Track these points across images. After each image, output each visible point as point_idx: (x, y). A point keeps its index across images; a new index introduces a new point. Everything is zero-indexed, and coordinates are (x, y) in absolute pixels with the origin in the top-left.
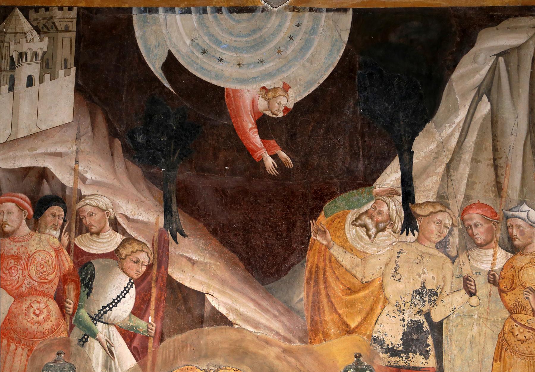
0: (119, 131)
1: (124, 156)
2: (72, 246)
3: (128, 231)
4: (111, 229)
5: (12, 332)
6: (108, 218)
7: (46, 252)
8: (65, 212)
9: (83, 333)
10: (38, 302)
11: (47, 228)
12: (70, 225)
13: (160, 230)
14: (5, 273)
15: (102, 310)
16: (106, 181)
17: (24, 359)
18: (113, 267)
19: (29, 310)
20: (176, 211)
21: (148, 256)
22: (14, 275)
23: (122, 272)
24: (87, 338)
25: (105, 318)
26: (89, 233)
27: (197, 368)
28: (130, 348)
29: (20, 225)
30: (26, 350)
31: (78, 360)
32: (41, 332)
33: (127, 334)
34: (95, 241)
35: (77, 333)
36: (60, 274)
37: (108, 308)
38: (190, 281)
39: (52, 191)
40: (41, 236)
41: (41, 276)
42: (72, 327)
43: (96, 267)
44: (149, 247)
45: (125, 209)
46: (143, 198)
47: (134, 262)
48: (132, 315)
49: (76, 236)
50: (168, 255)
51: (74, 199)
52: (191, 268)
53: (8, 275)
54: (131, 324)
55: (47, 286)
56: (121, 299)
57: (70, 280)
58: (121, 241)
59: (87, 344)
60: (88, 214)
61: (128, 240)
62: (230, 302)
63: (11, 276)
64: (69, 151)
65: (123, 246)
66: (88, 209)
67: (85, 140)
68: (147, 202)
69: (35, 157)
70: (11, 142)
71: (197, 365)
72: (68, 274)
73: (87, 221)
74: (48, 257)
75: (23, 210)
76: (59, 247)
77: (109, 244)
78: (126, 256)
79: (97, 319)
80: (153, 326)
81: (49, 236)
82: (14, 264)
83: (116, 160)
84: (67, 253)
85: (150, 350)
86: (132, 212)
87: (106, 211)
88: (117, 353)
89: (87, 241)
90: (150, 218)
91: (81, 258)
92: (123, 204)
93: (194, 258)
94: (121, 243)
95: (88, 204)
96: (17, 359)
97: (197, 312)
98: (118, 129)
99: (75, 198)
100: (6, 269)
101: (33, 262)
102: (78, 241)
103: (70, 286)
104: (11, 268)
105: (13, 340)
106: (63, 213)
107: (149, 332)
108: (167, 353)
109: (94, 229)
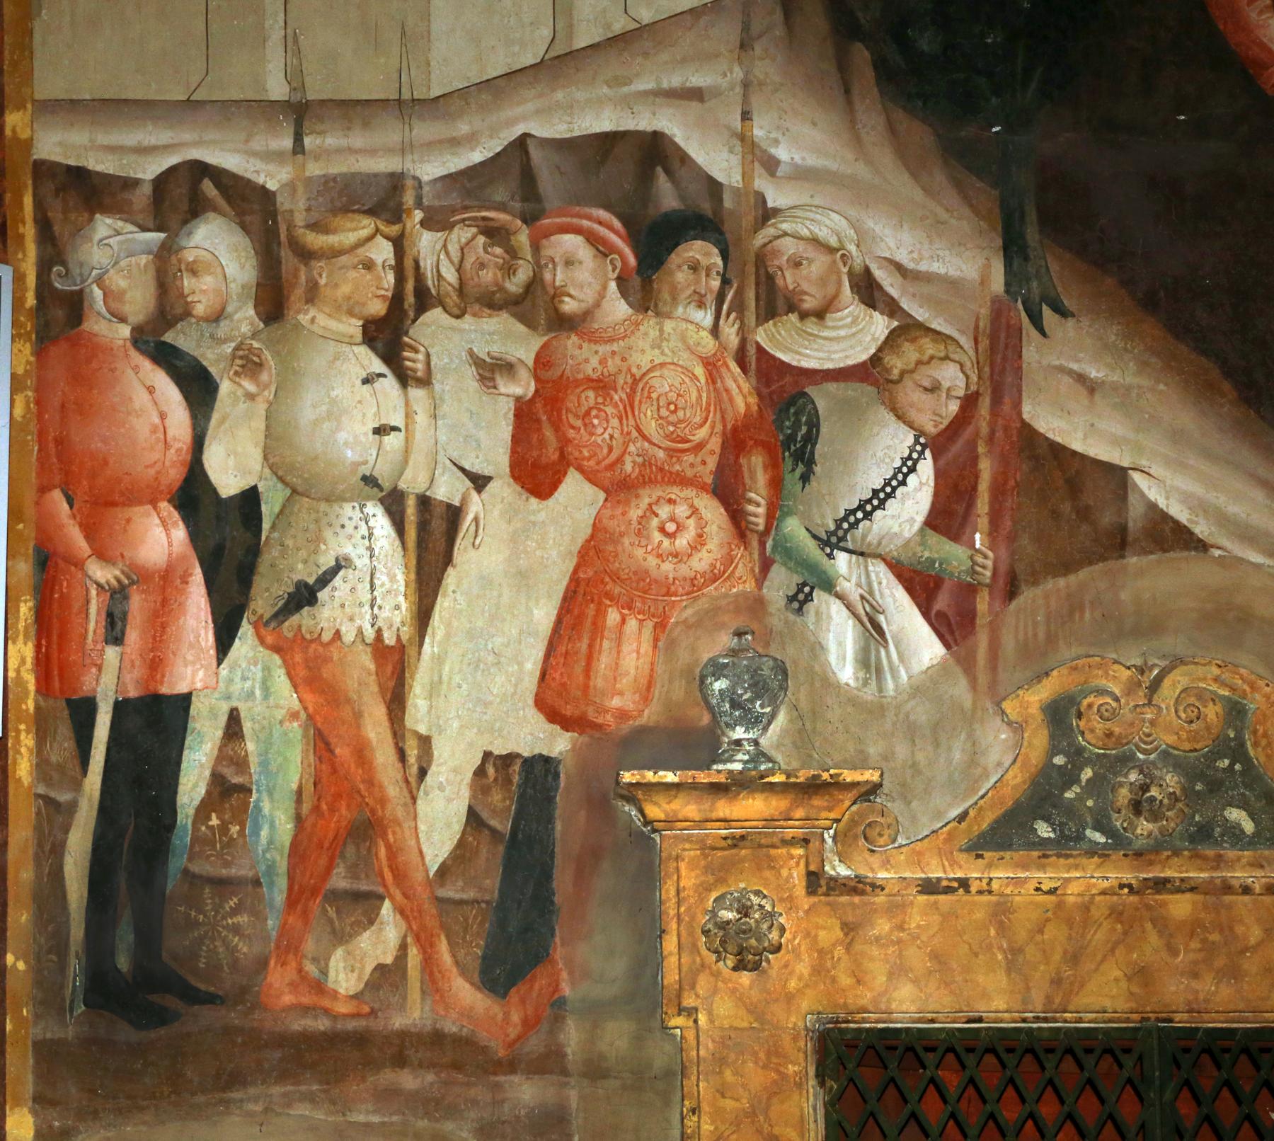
0: (863, 21)
2: (752, 351)
4: (856, 302)
5: (607, 579)
6: (845, 270)
8: (725, 256)
9: (797, 579)
10: (670, 501)
12: (740, 293)
13: (995, 301)
14: (573, 427)
15: (845, 519)
16: (832, 165)
17: (646, 647)
19: (648, 522)
21: (963, 372)
22: (600, 430)
23: (894, 418)
24: (811, 593)
25: (854, 540)
26: (796, 314)
27: (1116, 662)
28: (926, 614)
29: (602, 295)
30: (649, 625)
31: (791, 650)
32: (685, 579)
33: (917, 579)
34: (811, 334)
35: (781, 582)
36: (725, 426)
37: (860, 515)
39: (682, 198)
40: (661, 325)
42: (766, 565)
43: (821, 405)
44: (966, 347)
45: (892, 245)
46: (944, 215)
47: (926, 389)
48: (929, 532)
50: (1020, 368)
51: (747, 221)
52: (1086, 402)
53: (582, 431)
54: (927, 554)
55: (689, 458)
56: (894, 489)
57: (751, 443)
58: (887, 332)
59: (810, 608)
60: (788, 260)
61: (907, 330)
62: (1197, 489)
63: (592, 434)
64: (724, 83)
66: (789, 247)
67: (766, 50)
68: (953, 221)
69: (627, 103)
70: (556, 62)
71: (1114, 656)
72: (746, 427)
73: (789, 279)
74: (687, 380)
75: (606, 256)
76: (715, 354)
77: (853, 341)
78: (903, 373)
79: (832, 541)
80: (986, 557)
81: (684, 325)
82: (597, 403)
83: (859, 107)
84: (739, 370)
86: (912, 252)
87: (838, 250)
88: (894, 628)
89: (791, 336)
90: (964, 267)
92: (887, 231)
93: (1093, 374)
94: (887, 338)
95: (785, 234)
96: (628, 648)
97: (1107, 519)
98: (860, 14)
99: (751, 218)
100: (577, 416)
101: (646, 394)
103: (753, 458)
104: (588, 413)
106: (719, 261)
107: (977, 573)
108: (1030, 629)
109: (809, 303)
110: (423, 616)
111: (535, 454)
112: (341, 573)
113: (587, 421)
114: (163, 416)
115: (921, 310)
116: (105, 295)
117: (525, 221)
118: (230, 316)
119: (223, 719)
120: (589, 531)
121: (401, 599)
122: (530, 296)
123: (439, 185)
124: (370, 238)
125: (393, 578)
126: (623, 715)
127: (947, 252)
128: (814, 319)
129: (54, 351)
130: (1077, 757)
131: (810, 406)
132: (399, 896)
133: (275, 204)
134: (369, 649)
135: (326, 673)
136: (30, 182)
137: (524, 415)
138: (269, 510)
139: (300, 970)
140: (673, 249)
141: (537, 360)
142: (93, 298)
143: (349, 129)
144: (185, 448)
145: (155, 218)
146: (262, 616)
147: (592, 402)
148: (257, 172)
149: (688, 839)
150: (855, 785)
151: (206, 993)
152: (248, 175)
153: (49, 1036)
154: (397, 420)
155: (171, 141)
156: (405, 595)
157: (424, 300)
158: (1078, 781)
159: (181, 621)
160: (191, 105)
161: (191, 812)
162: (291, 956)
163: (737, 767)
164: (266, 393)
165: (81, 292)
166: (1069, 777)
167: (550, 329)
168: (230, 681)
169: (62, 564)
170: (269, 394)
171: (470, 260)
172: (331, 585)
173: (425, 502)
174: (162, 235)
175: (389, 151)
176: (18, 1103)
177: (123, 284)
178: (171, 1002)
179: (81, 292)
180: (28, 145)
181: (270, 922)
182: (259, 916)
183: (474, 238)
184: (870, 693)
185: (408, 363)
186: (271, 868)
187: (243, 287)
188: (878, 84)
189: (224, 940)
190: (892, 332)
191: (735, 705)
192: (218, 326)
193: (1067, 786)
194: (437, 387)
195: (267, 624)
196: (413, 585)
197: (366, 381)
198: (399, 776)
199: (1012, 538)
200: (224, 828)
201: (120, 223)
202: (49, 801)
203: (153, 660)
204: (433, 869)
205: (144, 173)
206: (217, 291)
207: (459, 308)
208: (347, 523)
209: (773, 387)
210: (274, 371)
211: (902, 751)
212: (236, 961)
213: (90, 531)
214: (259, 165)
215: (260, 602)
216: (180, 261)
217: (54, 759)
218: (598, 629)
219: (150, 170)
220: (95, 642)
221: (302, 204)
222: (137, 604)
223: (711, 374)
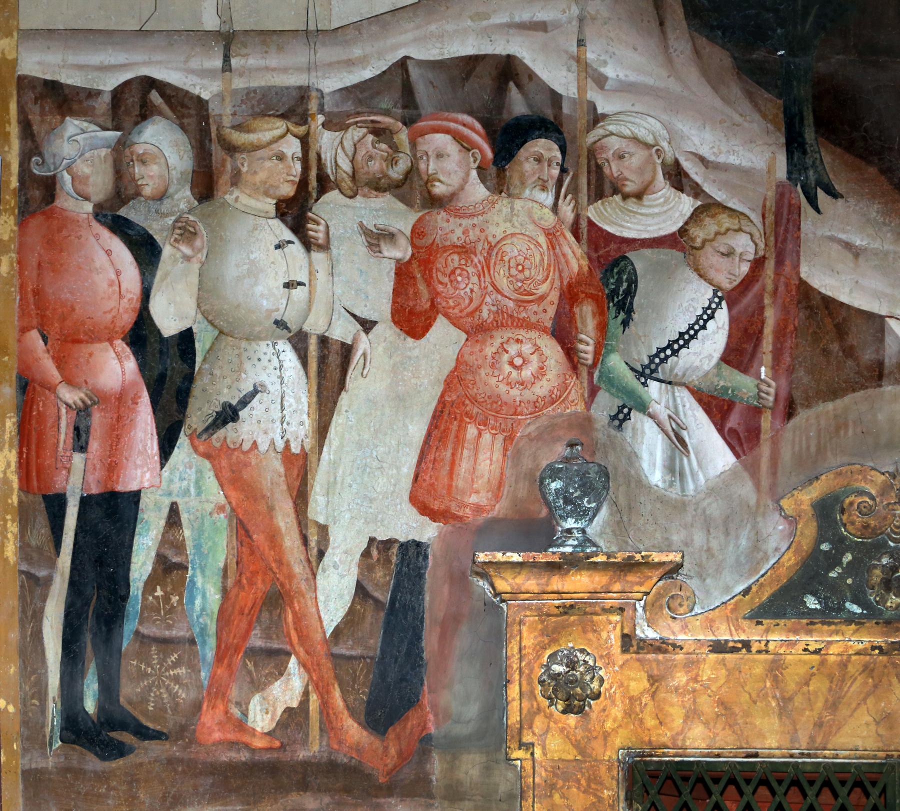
1: (688, 25)
2: (584, 224)
3: (707, 188)
4: (668, 186)
5: (467, 402)
6: (659, 161)
7: (527, 238)
10: (518, 341)
11: (525, 187)
12: (575, 178)
13: (780, 185)
14: (441, 283)
15: (657, 355)
16: (650, 81)
17: (497, 455)
18: (676, 265)
19: (500, 358)
20: (814, 143)
23: (697, 277)
24: (629, 413)
25: (664, 372)
26: (620, 196)
27: (873, 469)
28: (720, 430)
29: (465, 180)
30: (500, 438)
31: (612, 458)
32: (529, 402)
33: (714, 403)
36: (562, 282)
37: (669, 352)
38: (851, 291)
39: (530, 106)
40: (512, 203)
41: (520, 288)
42: (593, 391)
43: (639, 266)
46: (737, 118)
47: (723, 254)
48: (724, 365)
49: (591, 201)
50: (799, 237)
51: (582, 123)
52: (852, 265)
53: (449, 286)
54: (722, 383)
55: (534, 307)
56: (696, 332)
57: (583, 295)
58: (692, 210)
59: (628, 425)
60: (613, 154)
63: (456, 288)
64: (564, 18)
65: (696, 221)
66: (614, 143)
68: (746, 124)
69: (487, 33)
71: (871, 464)
72: (578, 284)
73: (613, 169)
74: (532, 246)
75: (469, 150)
76: (554, 227)
77: (664, 217)
78: (704, 242)
79: (645, 373)
80: (769, 386)
81: (530, 204)
82: (460, 264)
83: (671, 36)
84: (573, 239)
85: (765, 436)
86: (713, 147)
88: (694, 441)
89: (616, 213)
90: (754, 159)
91: (605, 248)
92: (693, 132)
93: (858, 243)
94: (692, 214)
95: (612, 134)
96: (483, 457)
97: (868, 356)
99: (584, 121)
100: (444, 274)
101: (499, 258)
102: (596, 212)
103: (584, 308)
104: (453, 272)
105: (471, 418)
106: (558, 155)
107: (763, 398)
108: (804, 442)
109: (630, 188)
110: (322, 431)
111: (411, 304)
112: (258, 396)
113: (452, 278)
115: (720, 193)
116: (73, 178)
117: (405, 124)
118: (171, 196)
120: (453, 364)
121: (305, 416)
122: (408, 181)
123: (337, 96)
124: (282, 136)
125: (298, 400)
126: (478, 509)
127: (741, 148)
128: (634, 200)
129: (35, 223)
130: (841, 544)
131: (630, 267)
132: (301, 651)
133: (207, 110)
134: (279, 456)
136: (15, 92)
137: (403, 273)
138: (201, 347)
140: (522, 146)
141: (413, 231)
142: (64, 182)
143: (266, 52)
144: (135, 297)
145: (113, 120)
146: (195, 430)
147: (456, 264)
148: (194, 85)
149: (529, 608)
150: (661, 564)
152: (185, 88)
154: (304, 278)
155: (127, 61)
156: (308, 414)
157: (325, 184)
158: (840, 563)
159: (132, 434)
163: (569, 550)
164: (199, 255)
165: (54, 177)
166: (833, 560)
167: (424, 207)
169: (38, 388)
170: (202, 256)
171: (361, 153)
172: (249, 406)
173: (324, 341)
174: (119, 133)
175: (299, 70)
177: (87, 170)
179: (54, 177)
183: (364, 137)
184: (674, 493)
185: (311, 233)
187: (182, 173)
188: (686, 19)
190: (696, 210)
191: (567, 501)
192: (162, 204)
193: (832, 568)
194: (334, 251)
196: (314, 406)
197: (278, 247)
198: (303, 557)
199: (791, 370)
201: (85, 124)
203: (110, 464)
204: (329, 632)
205: (105, 85)
206: (161, 176)
207: (352, 190)
208: (262, 357)
209: (601, 252)
210: (205, 238)
211: (699, 538)
213: (60, 362)
214: (195, 79)
215: (194, 419)
216: (132, 154)
218: (459, 441)
219: (109, 83)
220: (65, 450)
221: (229, 110)
223: (551, 242)
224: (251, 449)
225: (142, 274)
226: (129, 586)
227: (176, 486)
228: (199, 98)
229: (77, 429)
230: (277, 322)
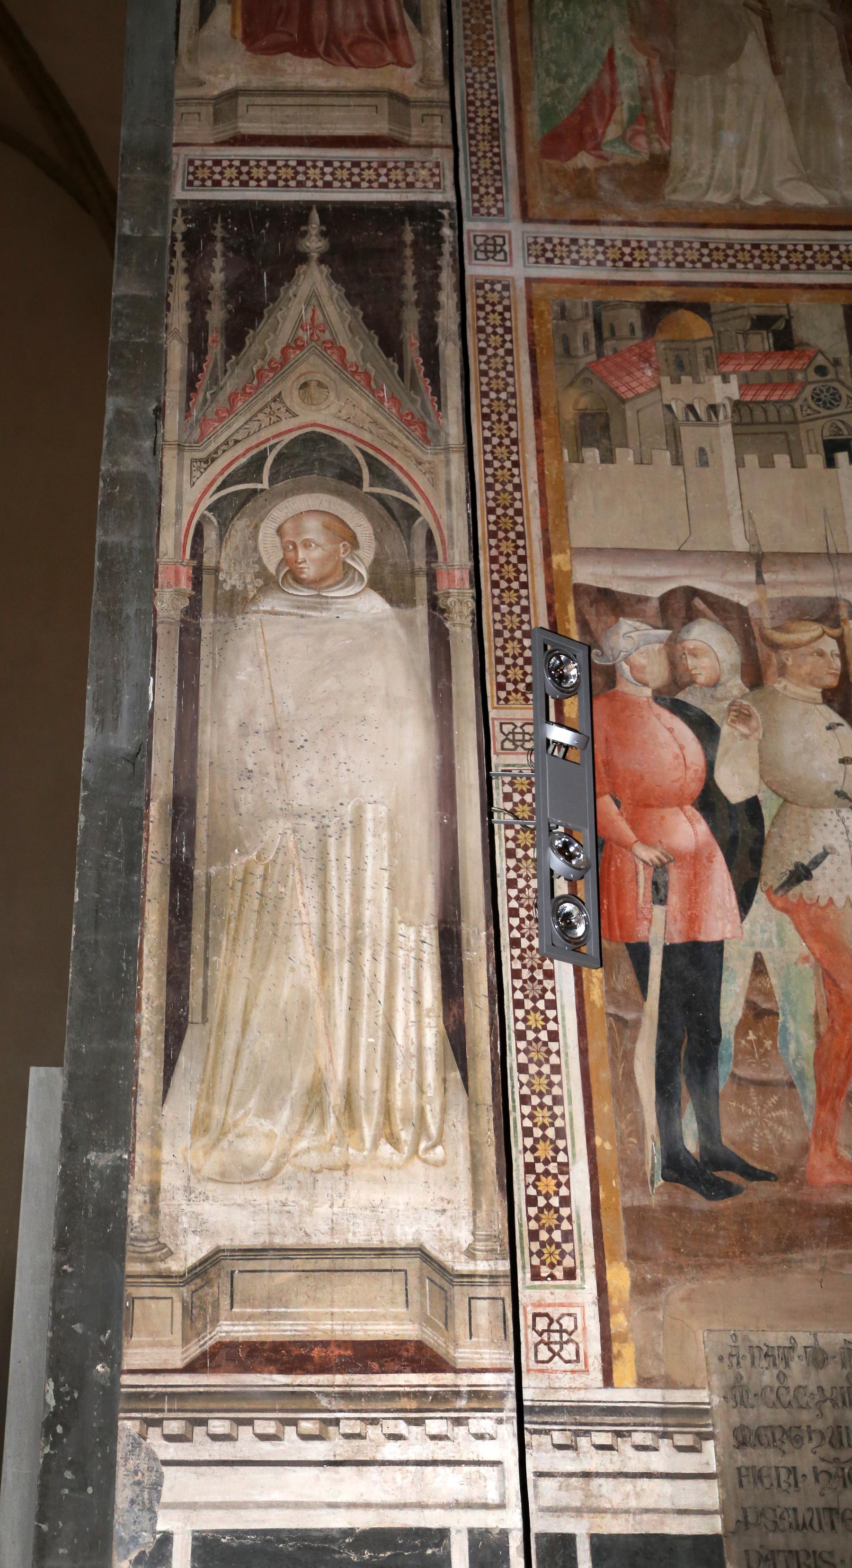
112: (829, 857)
114: (682, 748)
116: (631, 669)
118: (724, 684)
119: (750, 961)
124: (820, 637)
135: (826, 928)
136: (572, 597)
138: (768, 812)
139: (836, 1155)
144: (700, 769)
151: (761, 1171)
152: (726, 596)
153: (636, 1203)
159: (710, 889)
160: (681, 553)
161: (732, 1029)
162: (827, 1143)
164: (756, 734)
165: (614, 666)
168: (752, 933)
169: (614, 846)
170: (759, 734)
172: (821, 866)
174: (669, 632)
176: (615, 1257)
178: (734, 1178)
179: (614, 666)
180: (570, 573)
181: (806, 1117)
182: (796, 1110)
186: (801, 1074)
187: (731, 665)
189: (771, 1130)
195: (776, 892)
197: (829, 728)
200: (760, 1042)
201: (638, 624)
202: (618, 1018)
203: (690, 916)
208: (828, 823)
212: (783, 1146)
215: (770, 877)
216: (683, 648)
217: (620, 987)
219: (656, 591)
220: (645, 902)
221: (767, 615)
222: (675, 876)
224: (827, 906)
225: (705, 749)
226: (719, 1030)
227: (758, 937)
228: (739, 606)
229: (655, 884)
230: (838, 793)
